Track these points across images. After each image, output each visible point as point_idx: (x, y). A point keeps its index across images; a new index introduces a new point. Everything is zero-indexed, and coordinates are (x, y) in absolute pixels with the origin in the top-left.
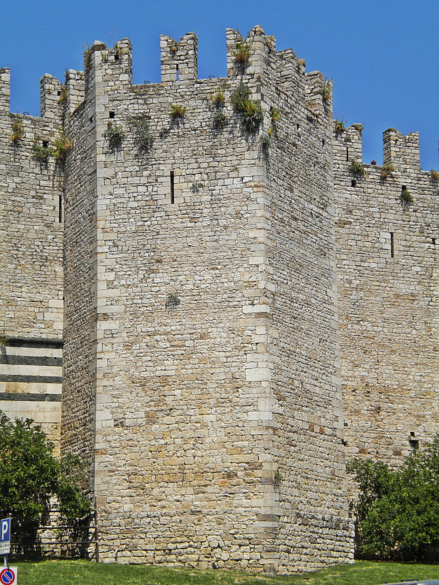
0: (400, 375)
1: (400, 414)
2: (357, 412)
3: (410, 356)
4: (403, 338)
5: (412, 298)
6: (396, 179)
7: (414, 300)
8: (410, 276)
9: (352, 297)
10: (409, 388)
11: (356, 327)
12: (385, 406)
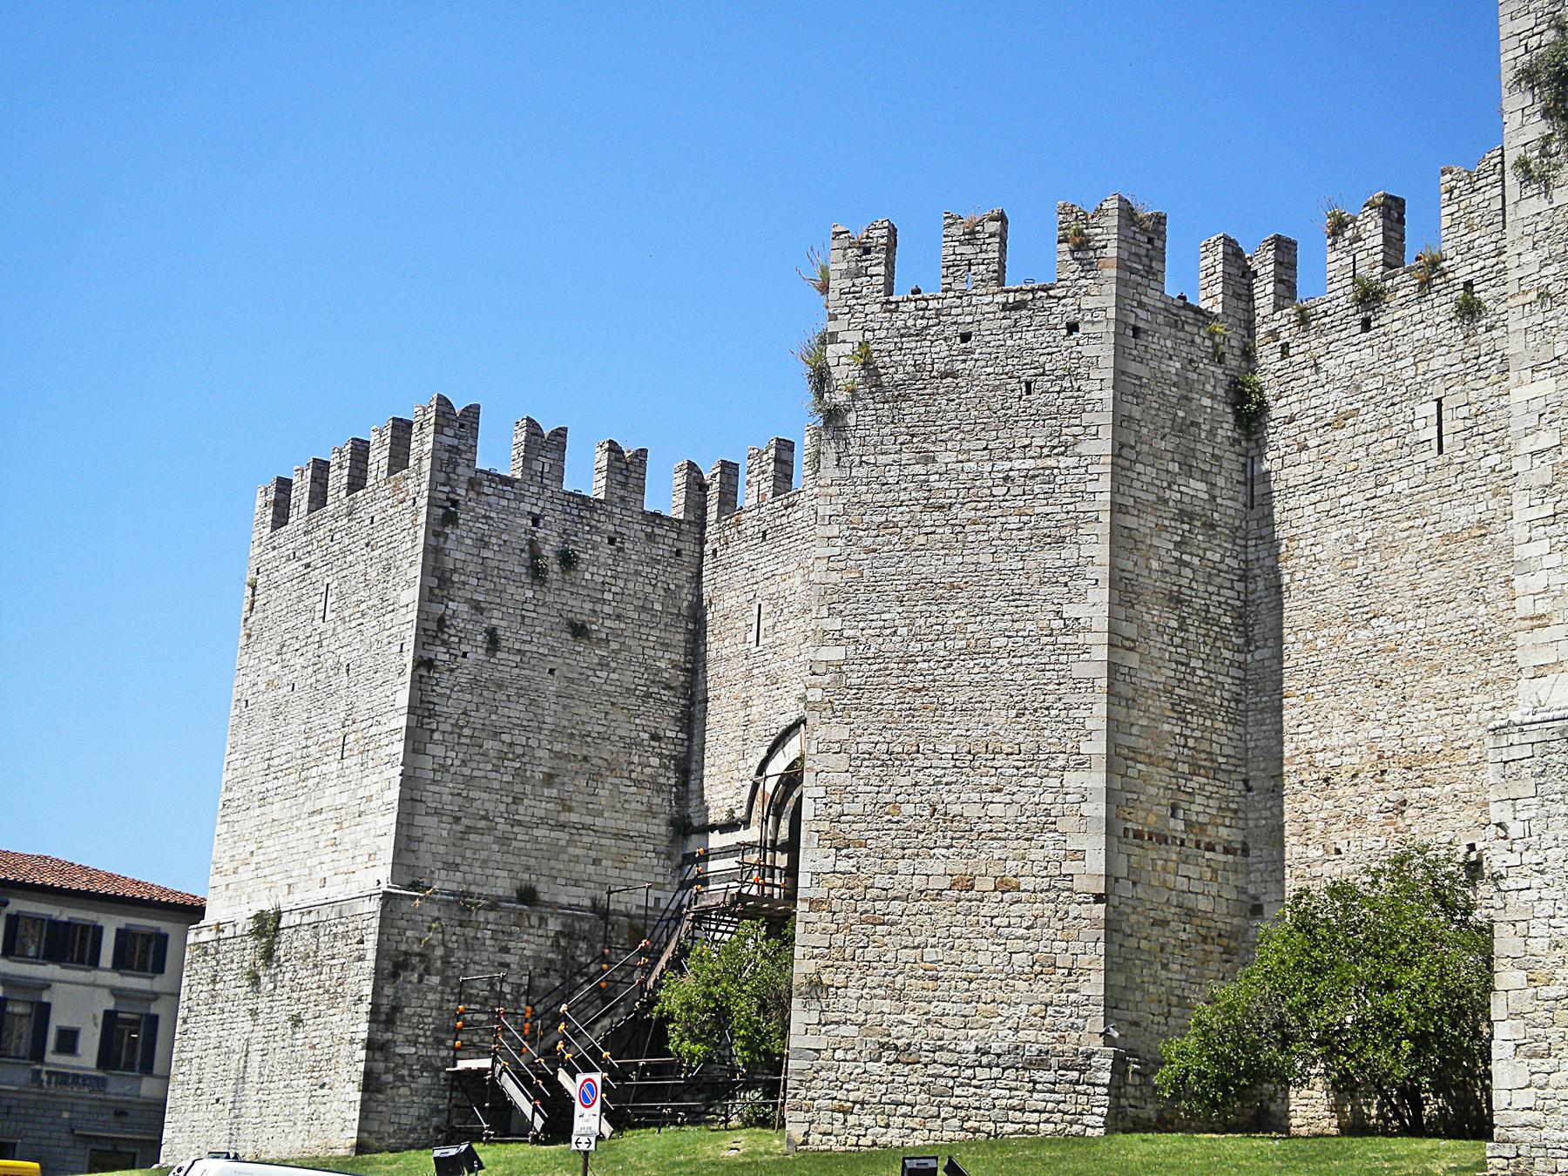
0: (1449, 718)
1: (1445, 808)
2: (1359, 819)
3: (1471, 668)
4: (1458, 631)
5: (1479, 533)
6: (1450, 276)
7: (1485, 535)
8: (1476, 482)
9: (1356, 572)
10: (1466, 744)
11: (1363, 634)
12: (1415, 794)
